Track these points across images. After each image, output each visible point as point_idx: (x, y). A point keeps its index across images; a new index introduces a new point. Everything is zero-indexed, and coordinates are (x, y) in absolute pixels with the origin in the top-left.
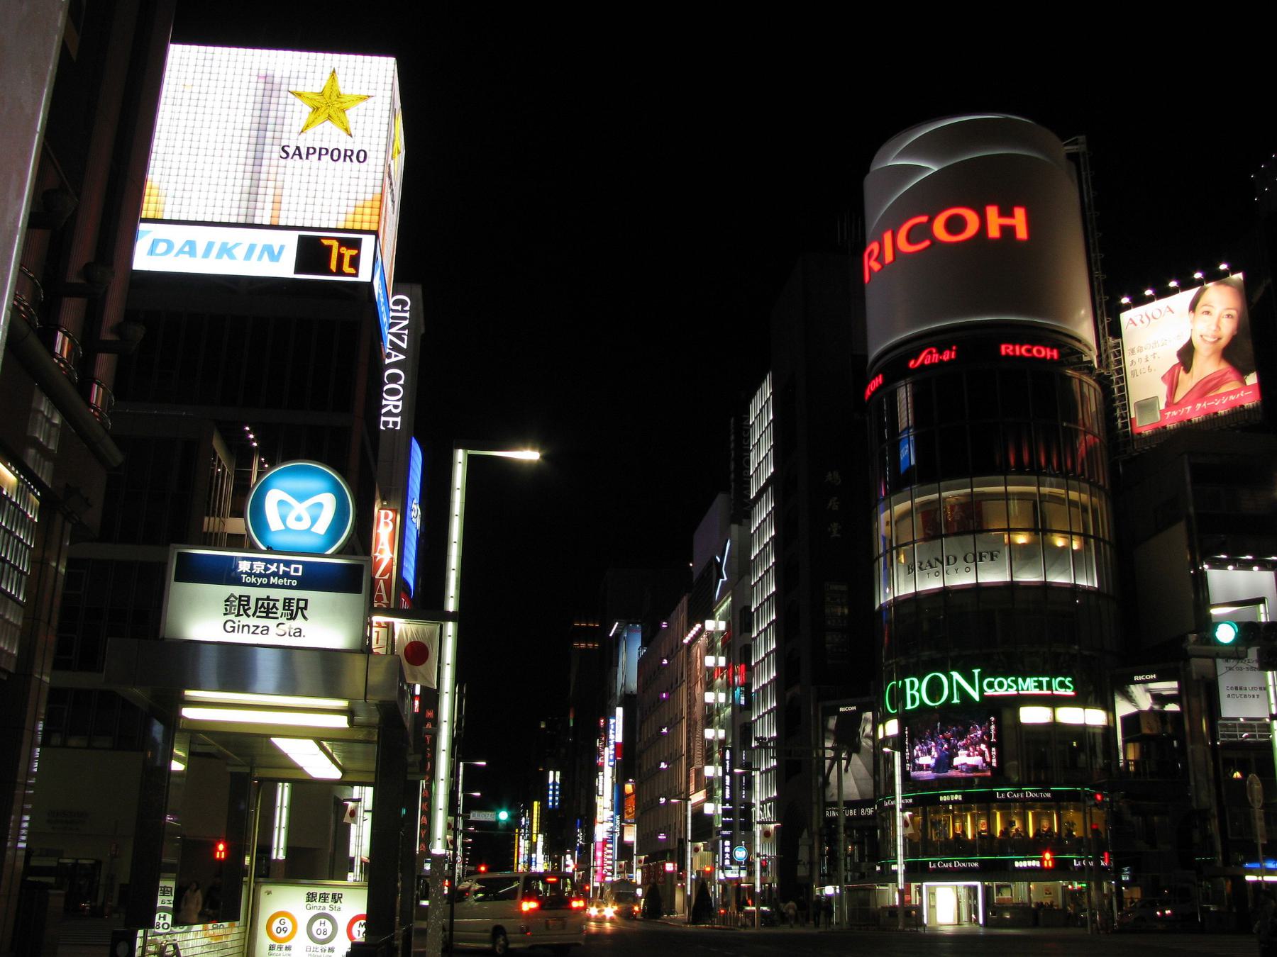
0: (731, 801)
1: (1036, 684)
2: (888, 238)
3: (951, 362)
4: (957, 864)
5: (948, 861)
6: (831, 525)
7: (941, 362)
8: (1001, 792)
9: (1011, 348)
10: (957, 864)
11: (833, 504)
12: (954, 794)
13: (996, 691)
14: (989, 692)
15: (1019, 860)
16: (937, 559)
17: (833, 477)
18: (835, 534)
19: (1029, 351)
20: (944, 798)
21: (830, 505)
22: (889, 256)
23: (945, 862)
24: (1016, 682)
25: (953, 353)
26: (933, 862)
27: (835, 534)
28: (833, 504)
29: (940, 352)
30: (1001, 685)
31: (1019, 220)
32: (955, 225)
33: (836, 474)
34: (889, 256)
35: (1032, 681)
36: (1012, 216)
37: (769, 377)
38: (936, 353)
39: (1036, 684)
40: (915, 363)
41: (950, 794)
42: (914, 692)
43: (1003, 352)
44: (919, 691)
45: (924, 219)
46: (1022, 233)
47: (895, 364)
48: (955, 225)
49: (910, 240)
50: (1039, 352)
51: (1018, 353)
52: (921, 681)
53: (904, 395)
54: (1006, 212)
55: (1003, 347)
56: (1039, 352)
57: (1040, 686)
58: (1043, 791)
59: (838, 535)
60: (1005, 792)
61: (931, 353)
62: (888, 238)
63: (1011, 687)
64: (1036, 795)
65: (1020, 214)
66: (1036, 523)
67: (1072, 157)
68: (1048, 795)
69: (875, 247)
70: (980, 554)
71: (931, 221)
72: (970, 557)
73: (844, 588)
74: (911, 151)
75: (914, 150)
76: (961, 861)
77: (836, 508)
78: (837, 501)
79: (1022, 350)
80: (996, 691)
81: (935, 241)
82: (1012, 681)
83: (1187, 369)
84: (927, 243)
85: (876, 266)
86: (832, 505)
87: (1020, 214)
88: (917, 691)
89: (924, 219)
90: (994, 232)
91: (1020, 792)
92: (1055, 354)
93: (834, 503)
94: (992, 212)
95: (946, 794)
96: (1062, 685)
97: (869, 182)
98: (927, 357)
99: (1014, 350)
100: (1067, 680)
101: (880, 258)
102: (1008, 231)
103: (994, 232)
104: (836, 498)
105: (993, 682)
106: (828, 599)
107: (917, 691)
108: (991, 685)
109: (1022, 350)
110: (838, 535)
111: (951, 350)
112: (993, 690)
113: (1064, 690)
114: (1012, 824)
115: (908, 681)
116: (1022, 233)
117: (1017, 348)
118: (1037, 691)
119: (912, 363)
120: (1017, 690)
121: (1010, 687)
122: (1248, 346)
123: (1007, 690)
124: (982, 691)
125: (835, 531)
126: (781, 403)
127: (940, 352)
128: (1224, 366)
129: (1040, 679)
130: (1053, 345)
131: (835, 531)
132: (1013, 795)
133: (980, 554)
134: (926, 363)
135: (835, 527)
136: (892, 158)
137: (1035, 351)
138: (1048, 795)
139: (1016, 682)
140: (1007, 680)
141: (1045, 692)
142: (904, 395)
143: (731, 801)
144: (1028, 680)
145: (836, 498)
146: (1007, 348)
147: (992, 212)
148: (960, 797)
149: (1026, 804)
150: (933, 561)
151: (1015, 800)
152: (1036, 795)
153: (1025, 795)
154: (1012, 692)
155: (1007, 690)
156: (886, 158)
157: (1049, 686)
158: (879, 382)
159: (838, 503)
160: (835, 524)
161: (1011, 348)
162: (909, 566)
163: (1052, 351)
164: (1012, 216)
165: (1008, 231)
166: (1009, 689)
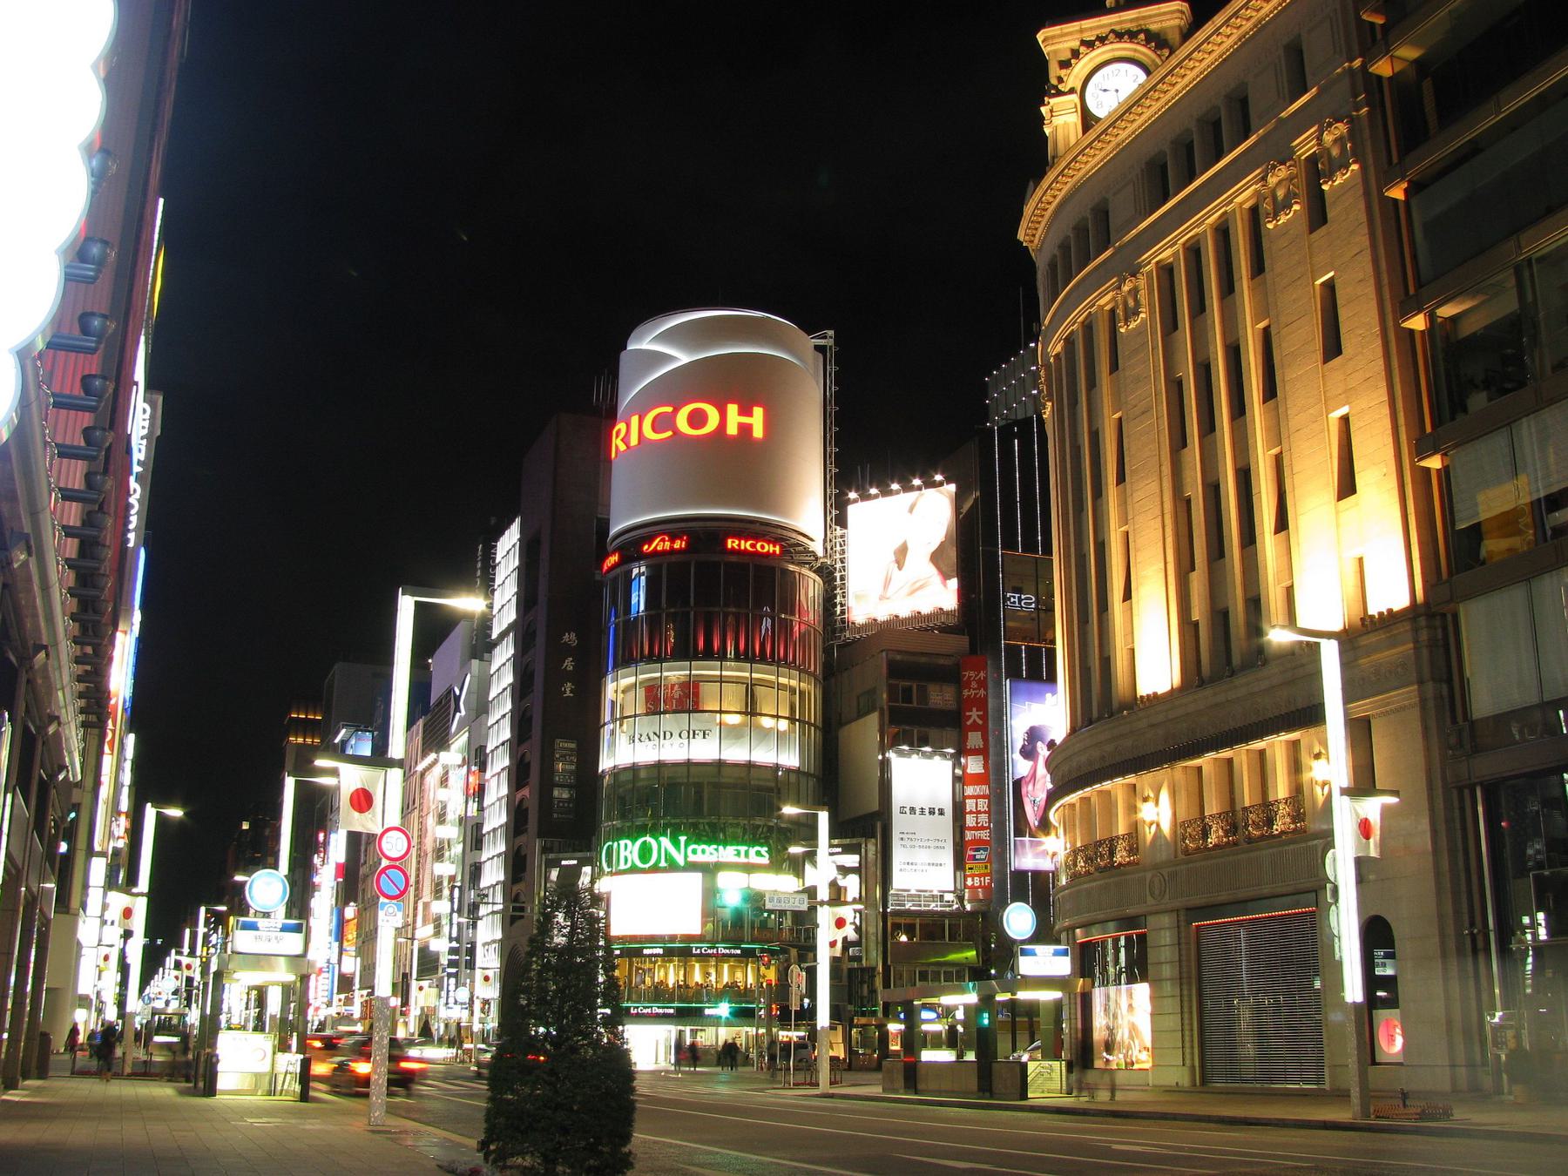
0: (458, 940)
2: (635, 420)
3: (680, 551)
5: (648, 1007)
7: (672, 551)
8: (697, 948)
9: (737, 542)
11: (569, 664)
14: (692, 858)
15: (709, 1008)
16: (655, 734)
17: (570, 638)
18: (568, 694)
19: (753, 546)
20: (646, 952)
22: (634, 441)
23: (645, 1008)
24: (717, 850)
27: (568, 694)
28: (569, 664)
29: (672, 541)
30: (703, 852)
31: (757, 419)
32: (697, 419)
33: (573, 635)
34: (634, 441)
36: (750, 415)
37: (518, 521)
40: (650, 546)
42: (627, 853)
43: (729, 546)
45: (669, 409)
46: (758, 432)
47: (632, 547)
48: (697, 419)
49: (655, 429)
50: (763, 547)
51: (743, 548)
52: (633, 843)
53: (639, 570)
54: (746, 411)
55: (730, 541)
56: (763, 547)
57: (738, 854)
58: (734, 948)
60: (701, 948)
61: (663, 540)
62: (635, 420)
64: (727, 951)
65: (758, 412)
66: (747, 707)
67: (820, 349)
68: (739, 952)
69: (622, 426)
70: (694, 732)
71: (676, 411)
72: (685, 734)
73: (573, 746)
74: (666, 337)
75: (668, 337)
76: (659, 1007)
79: (746, 545)
81: (676, 432)
83: (900, 568)
84: (669, 433)
85: (622, 447)
87: (758, 412)
89: (669, 409)
90: (732, 430)
91: (713, 948)
92: (777, 549)
94: (732, 409)
96: (758, 854)
97: (623, 355)
98: (660, 544)
99: (739, 545)
100: (764, 850)
101: (626, 440)
102: (745, 429)
103: (732, 430)
108: (694, 852)
109: (746, 545)
111: (682, 540)
115: (622, 843)
116: (758, 432)
117: (743, 542)
119: (646, 547)
122: (952, 554)
124: (686, 857)
126: (529, 549)
127: (672, 541)
128: (932, 570)
130: (774, 542)
133: (694, 732)
134: (659, 548)
135: (569, 686)
136: (645, 341)
137: (758, 547)
138: (739, 952)
139: (717, 850)
141: (742, 859)
142: (639, 570)
143: (458, 940)
144: (728, 847)
146: (733, 542)
147: (732, 409)
149: (722, 958)
150: (651, 735)
152: (727, 951)
156: (640, 339)
157: (747, 855)
161: (737, 542)
163: (774, 546)
164: (750, 415)
165: (745, 429)
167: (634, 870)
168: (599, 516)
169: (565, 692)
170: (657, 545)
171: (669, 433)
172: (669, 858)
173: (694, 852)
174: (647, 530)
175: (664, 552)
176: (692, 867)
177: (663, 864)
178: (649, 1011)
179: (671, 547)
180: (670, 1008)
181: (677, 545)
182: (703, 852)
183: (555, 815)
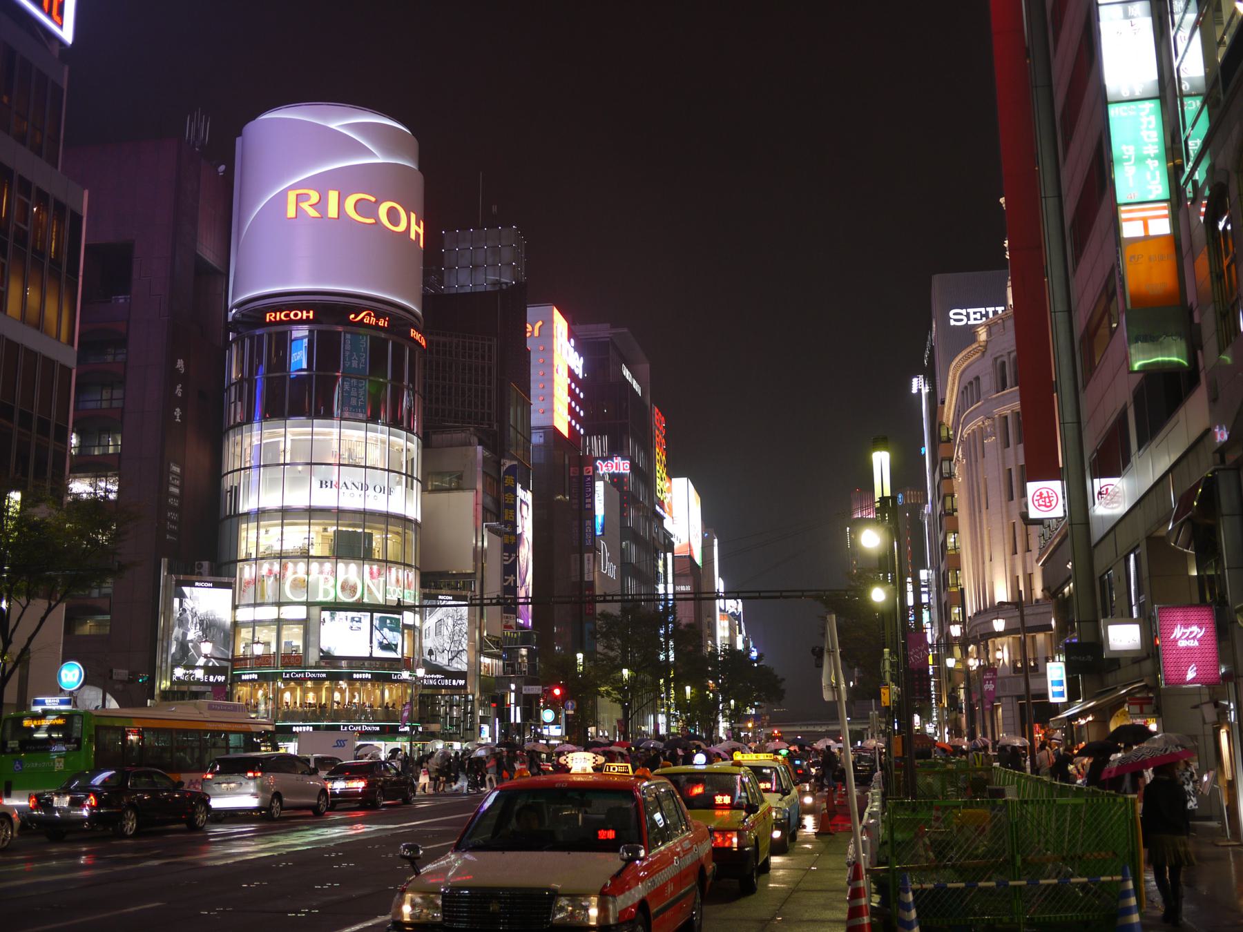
2: (333, 196)
5: (358, 725)
12: (365, 673)
28: (179, 391)
40: (356, 317)
41: (362, 673)
45: (373, 199)
48: (393, 216)
61: (369, 315)
71: (378, 203)
76: (367, 726)
77: (180, 395)
84: (372, 221)
89: (373, 199)
95: (359, 673)
103: (413, 236)
114: (354, 697)
127: (378, 320)
148: (370, 676)
150: (349, 485)
151: (310, 679)
158: (308, 317)
162: (321, 482)
170: (363, 318)
171: (372, 221)
174: (385, 307)
175: (368, 326)
178: (360, 728)
179: (377, 324)
181: (381, 323)
183: (168, 537)
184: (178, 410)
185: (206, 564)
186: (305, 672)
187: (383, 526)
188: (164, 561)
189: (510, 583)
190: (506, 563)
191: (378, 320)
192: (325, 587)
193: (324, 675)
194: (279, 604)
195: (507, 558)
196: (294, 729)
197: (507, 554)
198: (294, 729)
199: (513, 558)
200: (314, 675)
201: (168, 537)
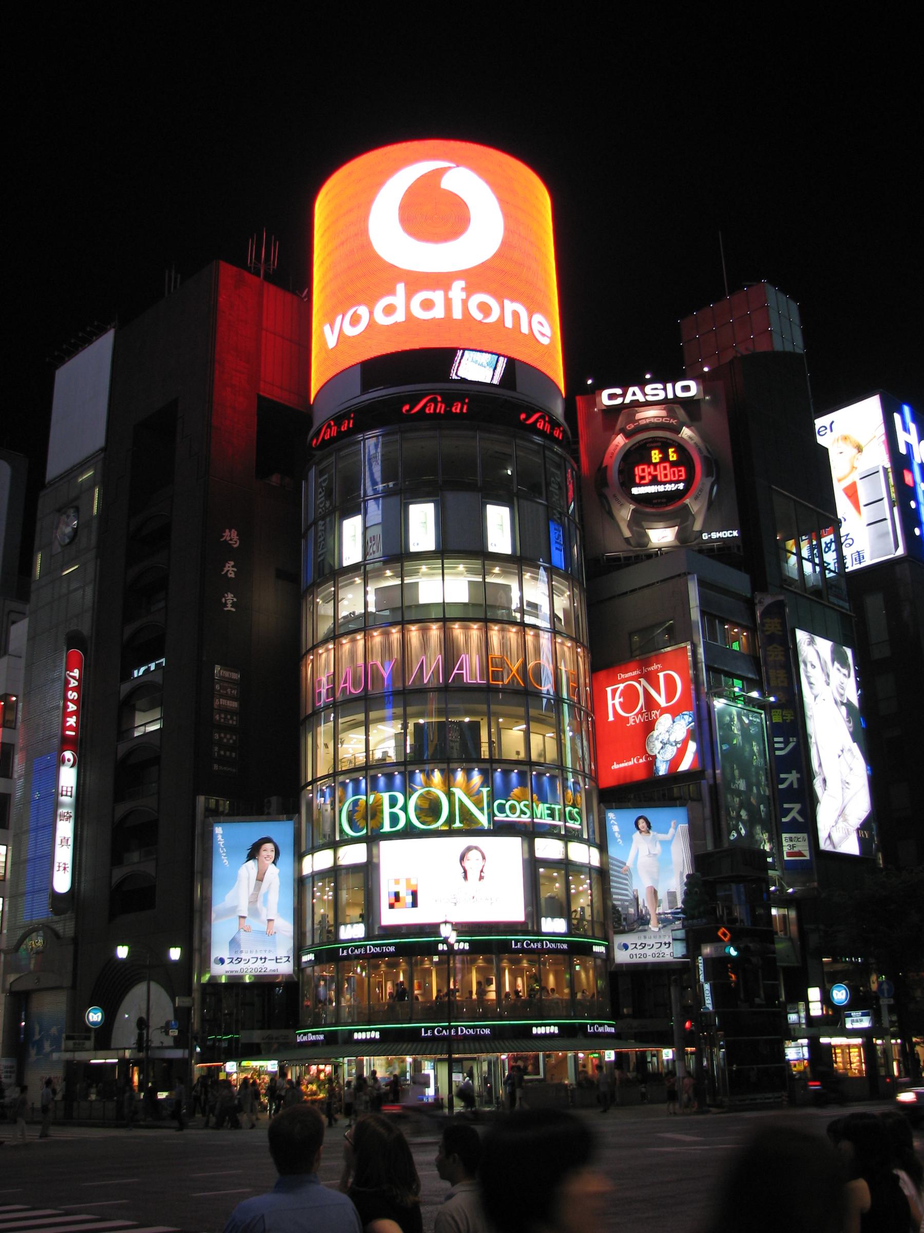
1: (549, 812)
4: (462, 1031)
6: (226, 595)
10: (462, 1031)
11: (230, 569)
13: (507, 816)
14: (500, 817)
15: (537, 1026)
17: (232, 537)
18: (229, 608)
21: (226, 569)
25: (465, 407)
26: (427, 1029)
28: (230, 569)
33: (234, 533)
35: (545, 809)
38: (442, 402)
39: (549, 812)
42: (396, 810)
44: (405, 808)
59: (233, 610)
63: (525, 813)
73: (236, 676)
76: (467, 1027)
77: (233, 576)
78: (233, 567)
80: (507, 816)
82: (525, 806)
86: (228, 571)
88: (401, 809)
93: (231, 569)
104: (232, 563)
105: (504, 805)
106: (217, 687)
107: (401, 809)
108: (502, 809)
110: (233, 610)
112: (505, 815)
113: (573, 822)
118: (549, 821)
120: (532, 817)
121: (523, 812)
123: (519, 817)
124: (491, 815)
125: (229, 602)
129: (553, 806)
131: (229, 602)
132: (530, 945)
140: (519, 804)
145: (232, 563)
153: (542, 945)
154: (525, 819)
155: (519, 817)
159: (235, 569)
160: (229, 593)
166: (522, 816)
167: (409, 832)
168: (261, 393)
169: (225, 605)
172: (466, 815)
173: (502, 809)
176: (502, 829)
177: (457, 825)
180: (486, 1027)
181: (457, 409)
182: (513, 808)
183: (216, 767)
184: (230, 596)
185: (274, 800)
186: (365, 946)
187: (484, 707)
188: (201, 799)
189: (792, 784)
190: (778, 753)
191: (449, 405)
192: (393, 810)
193: (392, 949)
194: (334, 846)
195: (781, 745)
196: (534, 1030)
197: (781, 739)
198: (534, 1030)
199: (791, 746)
200: (378, 949)
201: (216, 767)
